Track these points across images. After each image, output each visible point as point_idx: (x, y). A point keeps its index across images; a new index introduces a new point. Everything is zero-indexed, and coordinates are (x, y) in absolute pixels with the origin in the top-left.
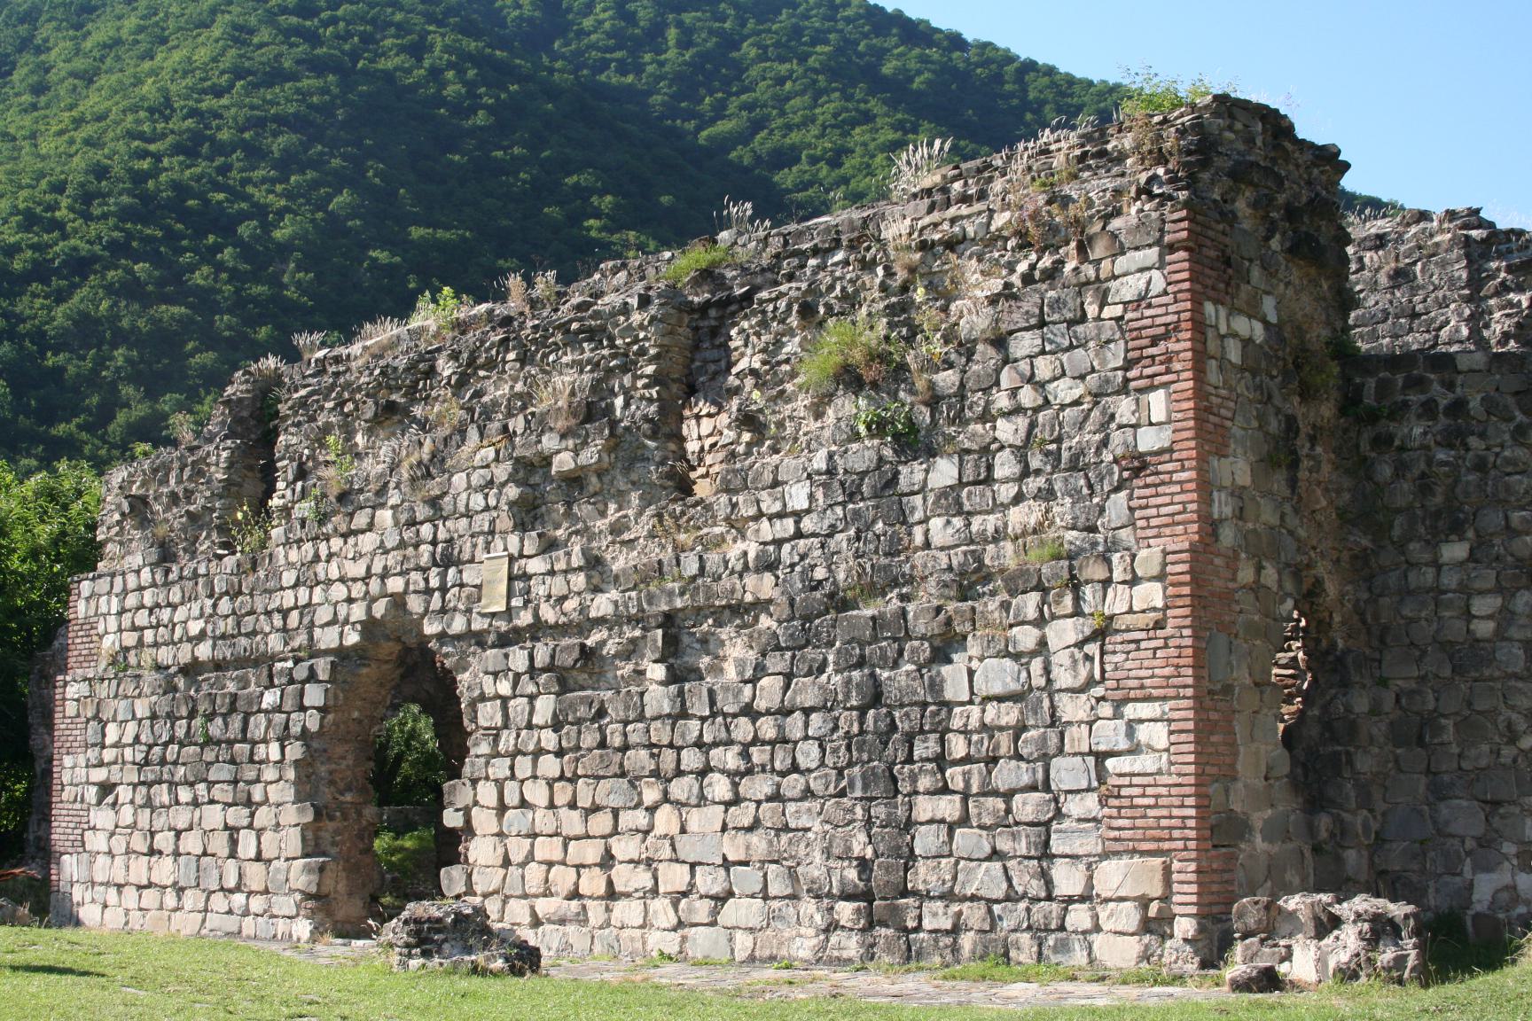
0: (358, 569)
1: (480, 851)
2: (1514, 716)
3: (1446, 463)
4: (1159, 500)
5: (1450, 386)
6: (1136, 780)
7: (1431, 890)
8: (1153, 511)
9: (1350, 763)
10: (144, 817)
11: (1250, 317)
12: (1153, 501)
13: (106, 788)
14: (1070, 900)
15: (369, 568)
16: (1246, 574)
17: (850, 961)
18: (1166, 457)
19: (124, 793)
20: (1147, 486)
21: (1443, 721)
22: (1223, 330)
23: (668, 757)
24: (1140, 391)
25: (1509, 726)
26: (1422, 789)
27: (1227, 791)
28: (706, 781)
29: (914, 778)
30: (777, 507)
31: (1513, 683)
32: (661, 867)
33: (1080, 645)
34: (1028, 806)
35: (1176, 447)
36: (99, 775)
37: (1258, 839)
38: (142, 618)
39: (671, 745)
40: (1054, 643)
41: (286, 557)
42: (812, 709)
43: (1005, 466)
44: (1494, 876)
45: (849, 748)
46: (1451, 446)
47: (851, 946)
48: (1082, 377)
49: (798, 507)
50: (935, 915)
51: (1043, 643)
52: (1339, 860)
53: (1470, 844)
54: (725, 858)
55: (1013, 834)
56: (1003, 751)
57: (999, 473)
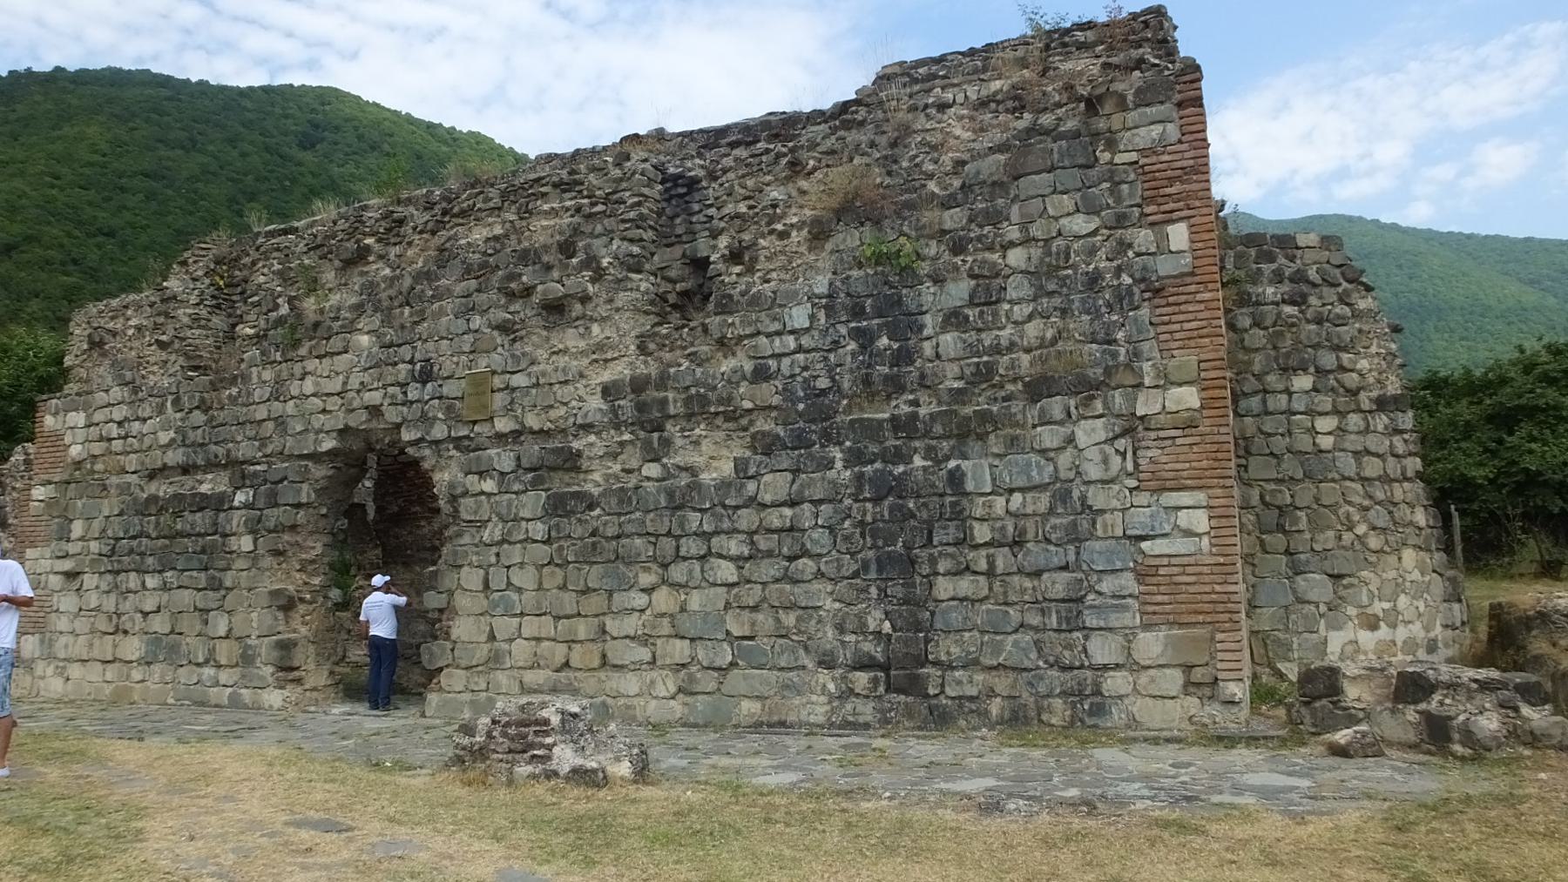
0: (335, 385)
1: (462, 628)
4: (1181, 317)
5: (1292, 259)
6: (1174, 561)
7: (1295, 646)
8: (1176, 327)
10: (110, 603)
12: (1174, 318)
13: (71, 575)
14: (1105, 668)
15: (345, 383)
17: (867, 726)
18: (1189, 280)
19: (90, 580)
20: (1169, 305)
21: (1299, 513)
23: (667, 544)
24: (1152, 224)
28: (707, 567)
29: (933, 561)
30: (776, 326)
31: (1348, 483)
32: (659, 642)
33: (1110, 441)
34: (1057, 584)
35: (1198, 271)
36: (67, 565)
38: (114, 431)
39: (669, 534)
40: (1082, 439)
41: (259, 377)
42: (821, 502)
43: (1018, 288)
44: (1342, 633)
45: (863, 535)
46: (1293, 303)
47: (867, 711)
48: (1097, 213)
49: (797, 326)
50: (959, 683)
51: (1071, 440)
53: (1323, 608)
54: (728, 633)
55: (1042, 610)
56: (1030, 536)
57: (1012, 293)
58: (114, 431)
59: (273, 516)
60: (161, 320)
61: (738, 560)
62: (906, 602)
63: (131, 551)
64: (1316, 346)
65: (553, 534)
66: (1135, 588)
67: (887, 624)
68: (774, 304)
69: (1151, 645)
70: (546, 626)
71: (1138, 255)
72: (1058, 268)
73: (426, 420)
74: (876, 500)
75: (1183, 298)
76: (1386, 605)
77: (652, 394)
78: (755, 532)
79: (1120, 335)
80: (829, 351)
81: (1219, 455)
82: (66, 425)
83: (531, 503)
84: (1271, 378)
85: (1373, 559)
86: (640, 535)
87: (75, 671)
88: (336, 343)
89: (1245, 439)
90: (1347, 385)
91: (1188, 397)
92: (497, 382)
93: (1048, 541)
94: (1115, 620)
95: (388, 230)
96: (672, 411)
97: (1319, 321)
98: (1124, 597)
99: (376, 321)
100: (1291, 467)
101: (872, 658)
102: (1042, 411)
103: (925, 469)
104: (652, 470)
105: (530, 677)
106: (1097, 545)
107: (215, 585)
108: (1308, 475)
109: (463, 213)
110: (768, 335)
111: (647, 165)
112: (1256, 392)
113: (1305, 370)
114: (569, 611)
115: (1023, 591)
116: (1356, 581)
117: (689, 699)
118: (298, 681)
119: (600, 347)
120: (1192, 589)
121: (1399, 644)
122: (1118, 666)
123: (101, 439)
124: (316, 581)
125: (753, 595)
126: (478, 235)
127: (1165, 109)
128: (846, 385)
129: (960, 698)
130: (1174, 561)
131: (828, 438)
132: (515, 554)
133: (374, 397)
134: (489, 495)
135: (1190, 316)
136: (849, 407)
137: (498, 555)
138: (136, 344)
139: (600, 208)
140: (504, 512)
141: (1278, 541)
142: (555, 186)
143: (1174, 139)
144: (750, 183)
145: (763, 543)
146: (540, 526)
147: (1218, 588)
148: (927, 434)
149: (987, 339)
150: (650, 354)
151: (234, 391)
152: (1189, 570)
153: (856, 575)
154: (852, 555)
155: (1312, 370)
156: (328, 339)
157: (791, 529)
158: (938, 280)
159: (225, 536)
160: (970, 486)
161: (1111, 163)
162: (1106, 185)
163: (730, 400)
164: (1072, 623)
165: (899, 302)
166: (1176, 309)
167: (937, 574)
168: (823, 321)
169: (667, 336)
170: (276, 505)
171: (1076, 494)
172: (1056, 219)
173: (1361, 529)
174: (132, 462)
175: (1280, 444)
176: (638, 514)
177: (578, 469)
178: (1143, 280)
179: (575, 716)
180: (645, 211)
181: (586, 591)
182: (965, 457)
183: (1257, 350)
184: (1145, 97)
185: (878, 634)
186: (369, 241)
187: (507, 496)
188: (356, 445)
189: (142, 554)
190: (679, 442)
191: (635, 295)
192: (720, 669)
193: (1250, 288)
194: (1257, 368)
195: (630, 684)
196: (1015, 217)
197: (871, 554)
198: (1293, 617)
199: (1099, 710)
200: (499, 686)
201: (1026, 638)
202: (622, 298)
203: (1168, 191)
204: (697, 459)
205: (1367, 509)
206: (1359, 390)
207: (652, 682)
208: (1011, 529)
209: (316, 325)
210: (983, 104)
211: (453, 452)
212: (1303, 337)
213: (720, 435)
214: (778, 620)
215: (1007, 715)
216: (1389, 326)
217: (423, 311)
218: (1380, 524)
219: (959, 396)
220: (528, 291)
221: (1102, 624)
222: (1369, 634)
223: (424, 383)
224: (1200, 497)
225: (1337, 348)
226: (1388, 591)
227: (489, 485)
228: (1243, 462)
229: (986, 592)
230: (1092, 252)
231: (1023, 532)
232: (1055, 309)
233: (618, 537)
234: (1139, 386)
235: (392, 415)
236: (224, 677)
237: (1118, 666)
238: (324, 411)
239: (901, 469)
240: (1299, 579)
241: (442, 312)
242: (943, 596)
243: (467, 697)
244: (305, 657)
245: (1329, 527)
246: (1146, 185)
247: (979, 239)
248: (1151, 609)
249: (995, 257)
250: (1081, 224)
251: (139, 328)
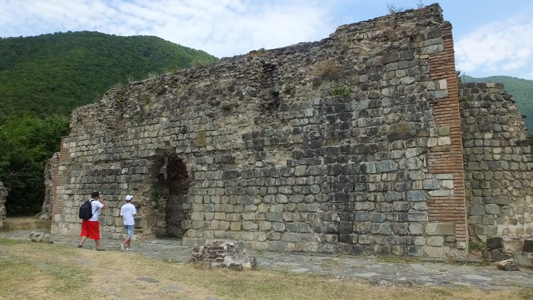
0: (155, 134)
1: (195, 216)
2: (506, 181)
3: (484, 112)
4: (444, 113)
5: (485, 92)
6: (441, 198)
7: (485, 230)
13: (71, 195)
14: (416, 235)
15: (158, 134)
17: (331, 253)
18: (447, 99)
19: (76, 197)
20: (439, 108)
21: (487, 182)
23: (264, 189)
24: (434, 80)
25: (505, 183)
29: (355, 197)
30: (302, 115)
31: (505, 172)
34: (399, 206)
35: (450, 96)
36: (69, 192)
38: (85, 148)
39: (264, 186)
40: (408, 155)
42: (316, 175)
43: (385, 102)
44: (503, 226)
45: (330, 187)
46: (485, 107)
47: (331, 248)
48: (414, 76)
49: (309, 115)
50: (364, 239)
51: (404, 155)
53: (496, 216)
54: (284, 220)
55: (393, 215)
56: (389, 189)
57: (383, 104)
58: (85, 148)
59: (134, 177)
60: (100, 112)
61: (288, 195)
62: (345, 210)
63: (89, 188)
64: (494, 123)
65: (225, 185)
66: (426, 208)
67: (339, 218)
68: (301, 108)
69: (432, 228)
70: (223, 216)
71: (428, 91)
72: (400, 95)
73: (184, 146)
74: (335, 175)
75: (445, 106)
76: (520, 216)
77: (259, 138)
78: (294, 186)
79: (422, 119)
80: (319, 124)
81: (458, 161)
82: (69, 146)
83: (218, 174)
85: (515, 199)
86: (255, 186)
87: (71, 226)
88: (155, 120)
89: (467, 155)
90: (505, 136)
91: (446, 141)
92: (208, 134)
93: (396, 190)
94: (419, 219)
95: (173, 83)
96: (266, 144)
97: (495, 114)
98: (422, 211)
99: (168, 113)
100: (484, 166)
101: (333, 229)
102: (394, 145)
103: (352, 165)
104: (259, 164)
105: (218, 233)
106: (413, 192)
107: (115, 199)
108: (490, 169)
109: (197, 77)
110: (299, 119)
111: (258, 61)
112: (471, 139)
113: (489, 131)
114: (230, 211)
115: (387, 208)
117: (270, 242)
118: (141, 232)
119: (242, 122)
120: (447, 208)
121: (525, 230)
122: (420, 235)
123: (80, 151)
124: (148, 199)
125: (293, 207)
126: (202, 84)
127: (439, 39)
128: (325, 136)
129: (364, 244)
130: (441, 198)
131: (319, 154)
132: (213, 191)
133: (167, 138)
134: (204, 171)
135: (447, 112)
136: (326, 143)
137: (207, 191)
138: (92, 120)
139: (242, 75)
140: (209, 177)
141: (478, 192)
142: (228, 68)
143: (442, 50)
144: (293, 66)
145: (296, 189)
146: (221, 182)
147: (457, 208)
148: (353, 153)
149: (375, 120)
150: (259, 125)
151: (122, 136)
152: (446, 201)
153: (328, 201)
154: (327, 194)
155: (492, 131)
156: (153, 119)
157: (306, 185)
158: (357, 100)
159: (119, 183)
160: (368, 171)
161: (419, 59)
162: (417, 66)
163: (285, 140)
164: (404, 219)
165: (344, 107)
166: (442, 110)
167: (356, 201)
168: (317, 114)
169: (264, 119)
170: (135, 174)
171: (406, 174)
172: (399, 78)
173: (510, 188)
174: (90, 159)
175: (479, 157)
176: (254, 179)
177: (234, 163)
178: (430, 99)
179: (232, 246)
180: (257, 76)
181: (236, 204)
182: (366, 161)
183: (472, 124)
184: (431, 36)
185: (335, 221)
186: (166, 87)
187: (210, 172)
188: (161, 154)
189: (92, 189)
190: (268, 154)
191: (254, 105)
192: (281, 232)
193: (469, 102)
194: (471, 130)
195: (250, 236)
196: (385, 78)
197: (333, 194)
198: (484, 219)
199: (413, 250)
200: (207, 236)
201: (388, 224)
202: (249, 106)
203: (439, 68)
204: (274, 160)
205: (513, 181)
206: (510, 138)
207: (258, 236)
208: (382, 186)
209: (149, 114)
210: (374, 39)
211: (193, 157)
212: (489, 119)
213: (282, 152)
214: (301, 216)
215: (380, 251)
216: (521, 115)
217: (184, 110)
218: (518, 186)
219: (364, 140)
220: (218, 103)
221: (414, 220)
222: (513, 226)
223: (184, 134)
224: (451, 176)
225: (502, 124)
226: (520, 211)
227: (204, 168)
228: (466, 163)
229: (373, 208)
230: (412, 90)
231: (387, 187)
232: (399, 110)
233: (247, 186)
234: (429, 136)
235: (173, 144)
236: (118, 230)
237: (420, 235)
238: (151, 143)
239: (344, 164)
240: (487, 205)
241: (190, 110)
242: (358, 209)
243: (196, 239)
244: (144, 224)
245: (498, 188)
246: (432, 66)
247: (372, 85)
248: (432, 215)
249: (378, 91)
250: (408, 80)
251: (93, 115)
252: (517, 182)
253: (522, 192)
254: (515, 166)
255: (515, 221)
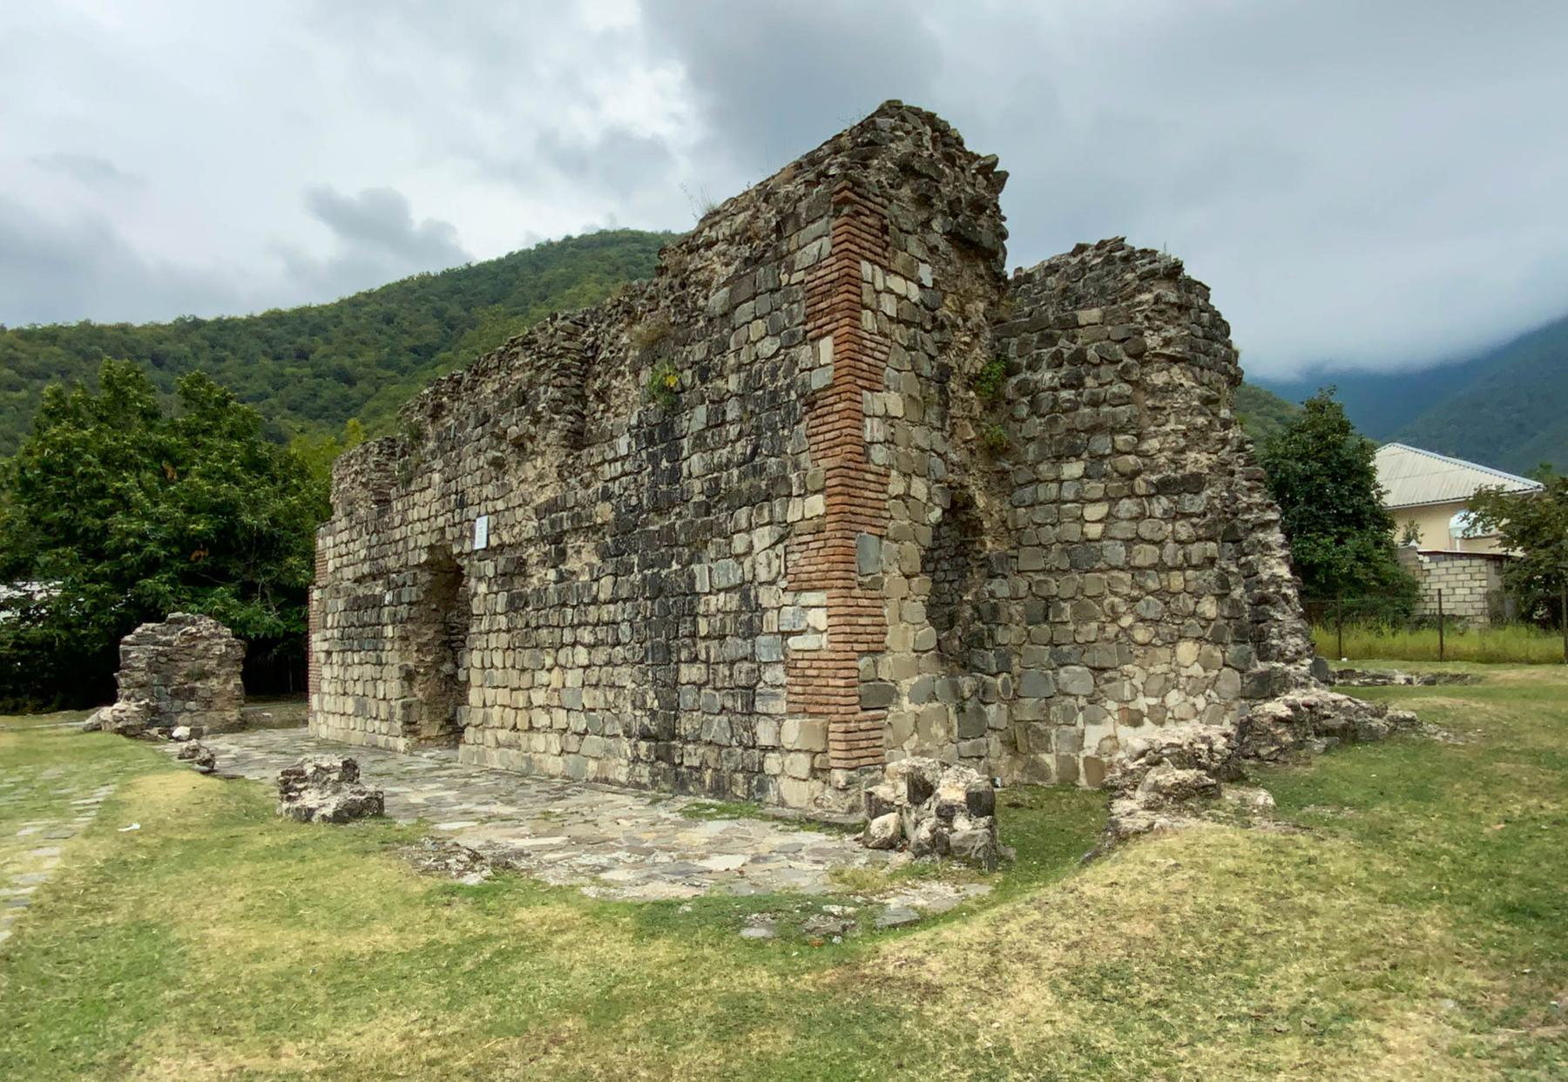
2: (1117, 600)
3: (1069, 400)
4: (824, 428)
5: (1073, 339)
7: (1053, 738)
9: (991, 637)
11: (906, 279)
16: (896, 486)
20: (818, 417)
22: (879, 285)
24: (812, 340)
25: (1113, 607)
26: (1046, 658)
27: (875, 663)
31: (1115, 573)
37: (905, 700)
46: (1072, 386)
52: (981, 714)
53: (1082, 702)
66: (784, 680)
75: (825, 410)
76: (1153, 701)
84: (1042, 467)
85: (1140, 651)
89: (1018, 530)
97: (1095, 403)
112: (1031, 482)
113: (1078, 457)
116: (1118, 675)
135: (829, 427)
143: (825, 253)
152: (815, 664)
173: (1127, 621)
175: (1049, 533)
205: (1136, 600)
218: (1150, 614)
222: (1130, 730)
225: (1114, 431)
226: (1155, 685)
228: (1014, 552)
229: (704, 678)
240: (1062, 671)
245: (1095, 619)
252: (1148, 603)
253: (1164, 630)
254: (1145, 555)
255: (1136, 716)
